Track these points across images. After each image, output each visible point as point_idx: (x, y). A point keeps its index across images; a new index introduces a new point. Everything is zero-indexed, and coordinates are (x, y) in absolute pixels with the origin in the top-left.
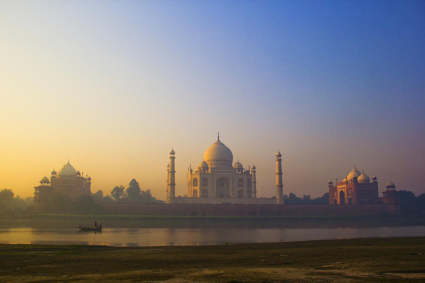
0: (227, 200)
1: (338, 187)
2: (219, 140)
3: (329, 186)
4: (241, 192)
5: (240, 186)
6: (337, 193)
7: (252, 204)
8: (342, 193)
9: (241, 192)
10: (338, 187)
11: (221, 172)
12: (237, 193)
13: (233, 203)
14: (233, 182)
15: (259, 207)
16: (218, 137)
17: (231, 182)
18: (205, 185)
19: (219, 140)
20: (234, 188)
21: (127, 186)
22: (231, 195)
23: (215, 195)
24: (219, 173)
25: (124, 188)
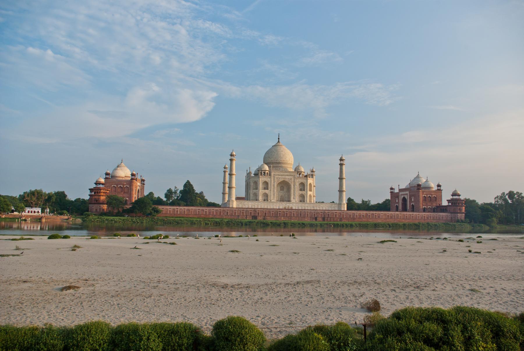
0: (288, 205)
1: (401, 193)
2: (279, 142)
3: (391, 192)
6: (398, 200)
8: (404, 200)
10: (401, 193)
11: (282, 175)
13: (294, 208)
14: (294, 186)
19: (279, 142)
21: (181, 188)
22: (292, 199)
23: (275, 199)
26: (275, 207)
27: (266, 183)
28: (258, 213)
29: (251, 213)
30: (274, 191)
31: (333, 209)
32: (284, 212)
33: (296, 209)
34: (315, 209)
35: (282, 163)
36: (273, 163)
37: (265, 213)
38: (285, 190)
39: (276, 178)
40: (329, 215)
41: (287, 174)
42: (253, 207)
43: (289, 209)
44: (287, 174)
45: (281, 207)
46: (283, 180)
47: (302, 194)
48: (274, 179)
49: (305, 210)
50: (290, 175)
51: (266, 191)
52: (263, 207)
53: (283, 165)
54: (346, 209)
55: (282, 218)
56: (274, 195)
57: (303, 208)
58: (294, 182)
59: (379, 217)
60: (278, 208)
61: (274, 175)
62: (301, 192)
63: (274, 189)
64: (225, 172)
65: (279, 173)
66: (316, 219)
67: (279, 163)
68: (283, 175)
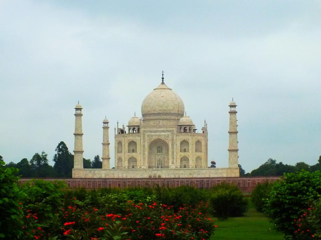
0: (156, 172)
2: (163, 83)
4: (185, 159)
5: (185, 151)
7: (191, 176)
9: (185, 159)
12: (179, 161)
13: (163, 176)
14: (173, 145)
16: (163, 78)
17: (170, 146)
18: (133, 151)
19: (163, 83)
20: (175, 154)
23: (147, 165)
24: (152, 134)
25: (46, 155)
27: (132, 144)
28: (110, 185)
30: (144, 154)
31: (220, 176)
36: (150, 114)
38: (164, 151)
39: (146, 137)
40: (208, 184)
41: (162, 129)
42: (107, 177)
43: (156, 179)
44: (162, 129)
46: (157, 137)
47: (185, 157)
48: (144, 138)
51: (134, 154)
52: (120, 176)
54: (238, 175)
56: (144, 158)
58: (173, 140)
61: (144, 131)
62: (183, 154)
63: (144, 151)
64: (106, 128)
65: (152, 129)
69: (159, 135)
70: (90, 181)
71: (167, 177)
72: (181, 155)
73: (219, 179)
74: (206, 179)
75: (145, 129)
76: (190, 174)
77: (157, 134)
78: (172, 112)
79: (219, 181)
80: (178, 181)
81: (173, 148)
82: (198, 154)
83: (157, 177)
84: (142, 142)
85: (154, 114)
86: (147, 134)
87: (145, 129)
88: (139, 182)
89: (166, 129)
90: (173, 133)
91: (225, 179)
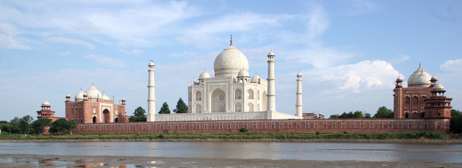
5: (240, 98)
11: (215, 83)
13: (213, 119)
14: (229, 94)
15: (237, 123)
16: (231, 41)
17: (227, 94)
18: (200, 99)
24: (213, 84)
26: (193, 120)
27: (198, 93)
28: (169, 126)
29: (162, 127)
32: (195, 124)
33: (215, 121)
34: (237, 119)
35: (229, 69)
37: (176, 127)
40: (246, 126)
41: (221, 80)
44: (221, 80)
45: (199, 119)
46: (216, 87)
47: (238, 103)
48: (207, 88)
49: (225, 121)
50: (224, 82)
51: (199, 102)
53: (228, 71)
55: (194, 131)
57: (223, 119)
58: (229, 89)
59: (312, 126)
60: (196, 120)
62: (237, 101)
65: (212, 81)
66: (230, 130)
67: (223, 69)
68: (217, 82)
69: (218, 86)
70: (155, 124)
71: (216, 119)
72: (235, 102)
73: (254, 121)
74: (244, 122)
75: (208, 81)
76: (235, 117)
77: (217, 84)
78: (234, 67)
79: (255, 123)
80: (221, 123)
81: (229, 96)
82: (251, 101)
83: (209, 120)
84: (205, 91)
85: (220, 69)
86: (209, 85)
87: (208, 81)
88: (191, 124)
89: (223, 80)
90: (229, 84)
91: (260, 121)
